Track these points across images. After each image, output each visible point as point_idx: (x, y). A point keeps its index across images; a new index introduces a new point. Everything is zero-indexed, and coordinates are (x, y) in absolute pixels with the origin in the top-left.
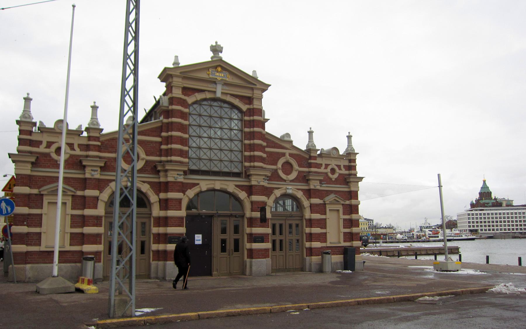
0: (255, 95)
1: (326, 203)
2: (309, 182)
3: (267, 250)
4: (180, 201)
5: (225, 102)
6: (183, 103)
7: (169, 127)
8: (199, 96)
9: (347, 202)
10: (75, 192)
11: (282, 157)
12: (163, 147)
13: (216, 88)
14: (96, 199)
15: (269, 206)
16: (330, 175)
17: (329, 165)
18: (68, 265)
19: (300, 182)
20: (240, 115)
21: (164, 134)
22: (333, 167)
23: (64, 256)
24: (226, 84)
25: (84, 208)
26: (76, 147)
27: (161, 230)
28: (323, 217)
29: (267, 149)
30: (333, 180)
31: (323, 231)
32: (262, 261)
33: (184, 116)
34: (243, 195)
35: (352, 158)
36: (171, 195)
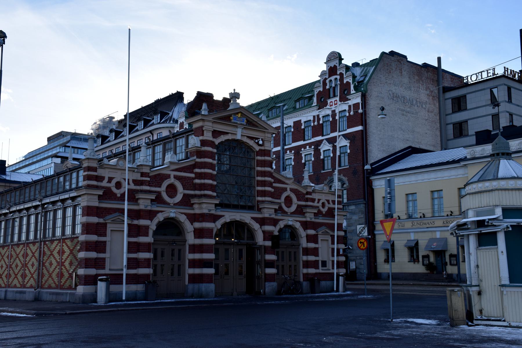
8: (223, 138)
13: (237, 132)
14: (147, 228)
16: (321, 208)
17: (320, 199)
21: (197, 170)
25: (138, 235)
27: (197, 256)
29: (274, 185)
30: (324, 213)
34: (256, 226)
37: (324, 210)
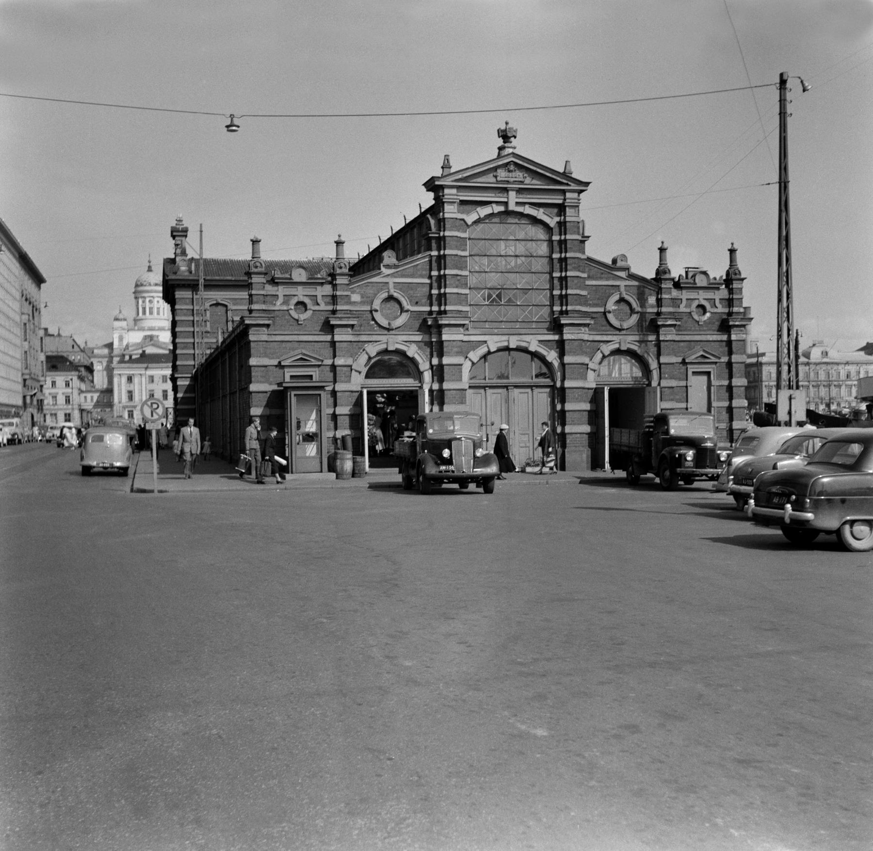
0: (567, 201)
5: (521, 215)
13: (508, 198)
22: (700, 304)
26: (320, 300)
29: (588, 283)
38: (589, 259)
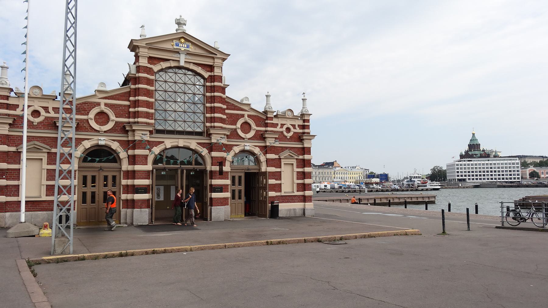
0: (215, 63)
1: (281, 158)
2: (265, 140)
3: (226, 199)
4: (146, 157)
5: (188, 69)
6: (149, 71)
7: (137, 92)
8: (164, 65)
9: (301, 157)
10: (50, 150)
11: (241, 118)
12: (131, 110)
15: (228, 161)
16: (285, 133)
18: (45, 212)
19: (258, 140)
20: (202, 81)
21: (132, 98)
22: (288, 127)
23: (32, 205)
24: (189, 54)
26: (50, 110)
27: (130, 182)
28: (278, 170)
29: (227, 111)
30: (288, 137)
31: (278, 182)
32: (221, 208)
33: (149, 82)
34: (204, 152)
35: (306, 118)
36: (138, 152)
37: (289, 135)
38: (227, 97)
